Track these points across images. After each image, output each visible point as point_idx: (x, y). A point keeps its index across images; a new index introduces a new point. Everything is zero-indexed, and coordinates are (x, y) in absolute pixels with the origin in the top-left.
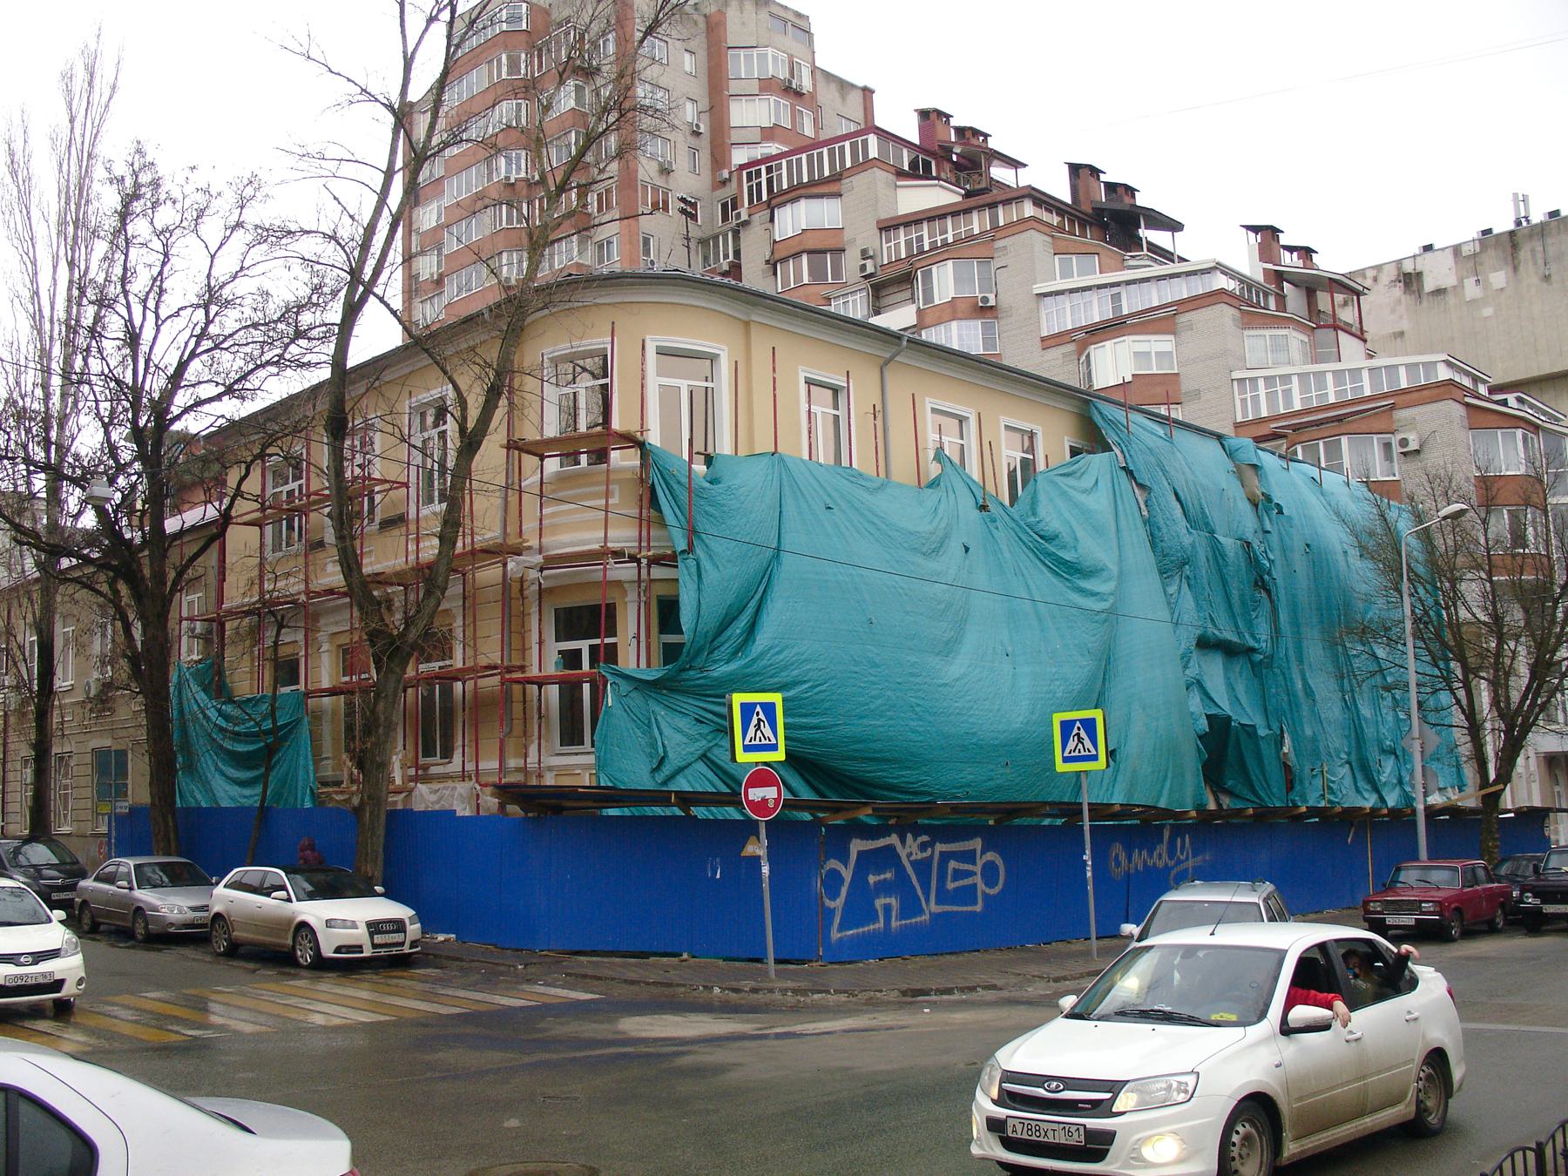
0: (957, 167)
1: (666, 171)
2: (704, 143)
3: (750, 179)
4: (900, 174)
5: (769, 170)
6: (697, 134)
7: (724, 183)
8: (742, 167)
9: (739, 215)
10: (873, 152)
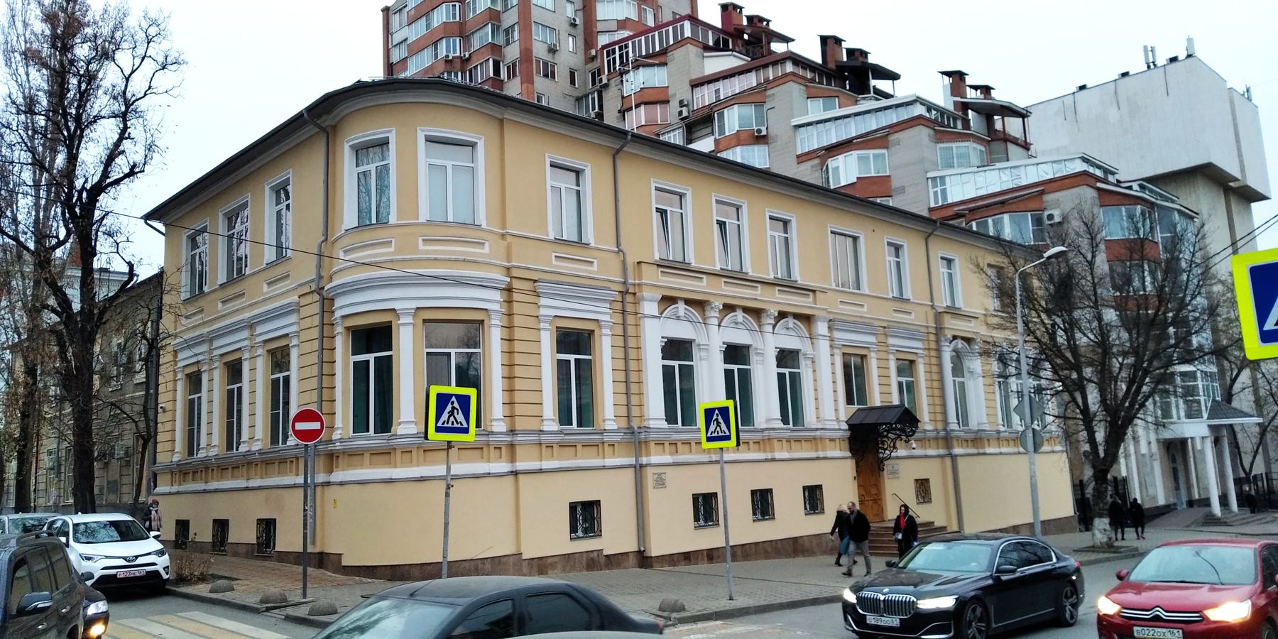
0: (747, 43)
1: (553, 50)
2: (580, 31)
3: (608, 56)
4: (707, 48)
5: (621, 49)
6: (574, 25)
7: (593, 59)
8: (604, 47)
9: (601, 80)
10: (688, 33)
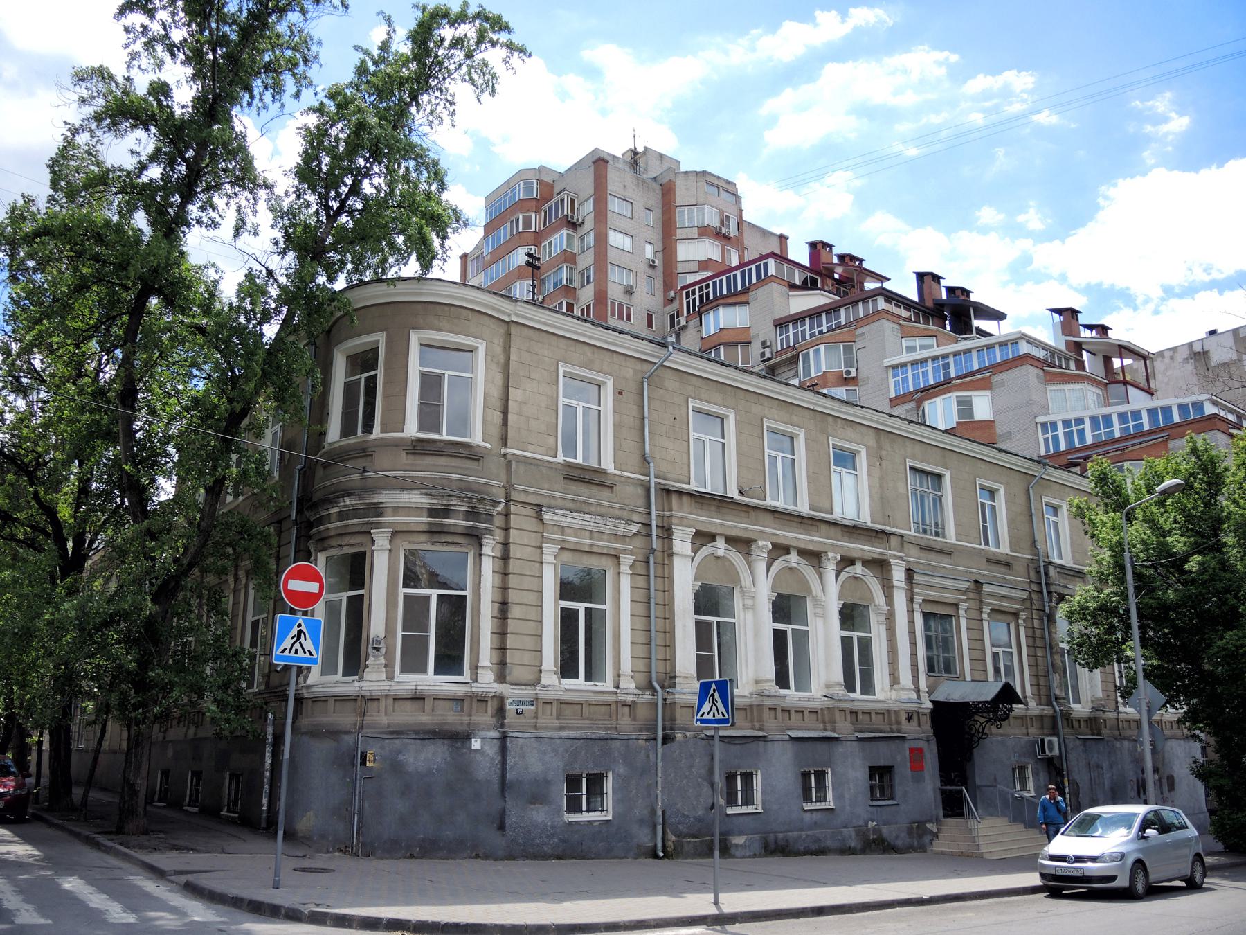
0: (838, 282)
1: (629, 292)
2: (659, 273)
3: (688, 296)
4: (793, 286)
5: (701, 289)
6: (652, 266)
7: (672, 300)
8: (683, 288)
9: (679, 322)
10: (772, 271)
